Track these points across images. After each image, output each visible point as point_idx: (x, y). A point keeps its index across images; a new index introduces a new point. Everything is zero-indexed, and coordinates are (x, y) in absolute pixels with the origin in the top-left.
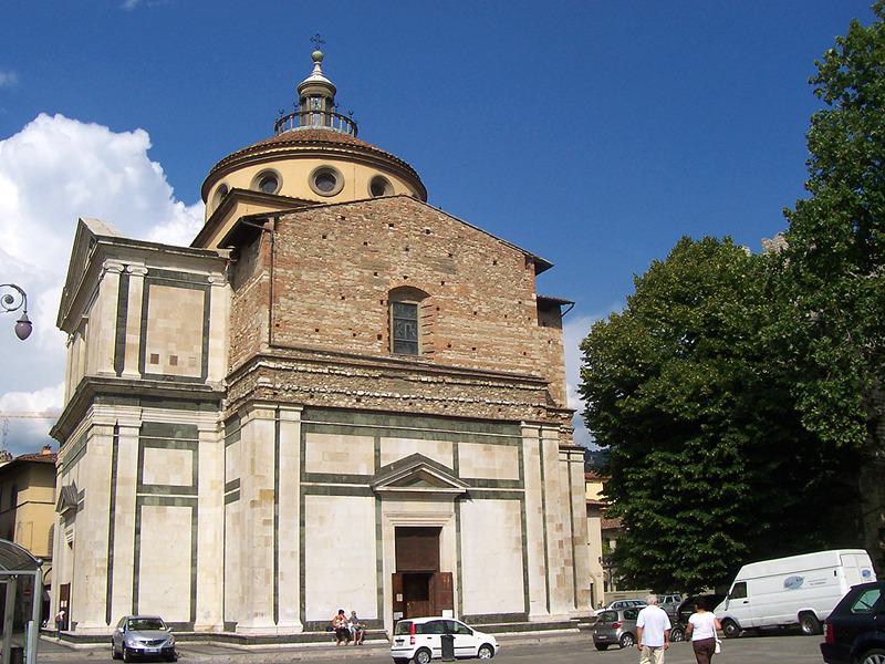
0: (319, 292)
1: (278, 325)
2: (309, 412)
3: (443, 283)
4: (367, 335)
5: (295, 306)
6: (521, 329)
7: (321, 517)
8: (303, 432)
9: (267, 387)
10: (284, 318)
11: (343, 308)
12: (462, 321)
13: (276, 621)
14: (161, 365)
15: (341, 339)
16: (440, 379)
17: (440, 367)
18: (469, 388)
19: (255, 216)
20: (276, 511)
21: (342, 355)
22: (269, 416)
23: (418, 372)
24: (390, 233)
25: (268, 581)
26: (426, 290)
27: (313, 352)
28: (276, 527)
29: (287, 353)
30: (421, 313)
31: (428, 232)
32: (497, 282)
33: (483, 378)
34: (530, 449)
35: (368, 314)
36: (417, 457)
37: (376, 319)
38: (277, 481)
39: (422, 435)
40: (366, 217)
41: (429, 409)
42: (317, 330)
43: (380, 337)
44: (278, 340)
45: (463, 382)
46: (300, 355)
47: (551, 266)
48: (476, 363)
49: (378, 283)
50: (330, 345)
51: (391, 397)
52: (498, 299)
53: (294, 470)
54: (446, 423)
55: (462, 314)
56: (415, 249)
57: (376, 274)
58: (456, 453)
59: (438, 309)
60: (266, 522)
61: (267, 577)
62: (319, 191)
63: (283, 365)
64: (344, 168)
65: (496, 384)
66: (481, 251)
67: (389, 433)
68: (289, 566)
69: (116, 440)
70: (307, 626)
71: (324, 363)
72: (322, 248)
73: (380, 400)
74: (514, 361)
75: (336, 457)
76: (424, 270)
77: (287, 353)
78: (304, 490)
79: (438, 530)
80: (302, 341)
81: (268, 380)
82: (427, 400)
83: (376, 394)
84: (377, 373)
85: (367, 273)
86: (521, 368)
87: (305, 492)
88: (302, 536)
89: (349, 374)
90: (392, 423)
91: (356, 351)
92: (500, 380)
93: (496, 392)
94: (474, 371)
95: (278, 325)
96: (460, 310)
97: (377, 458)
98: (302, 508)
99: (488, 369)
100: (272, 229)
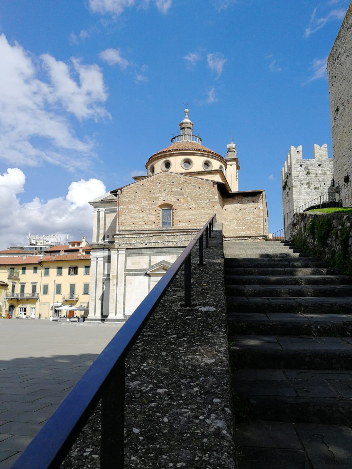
0: (134, 211)
3: (178, 200)
4: (150, 223)
6: (209, 211)
8: (126, 256)
9: (117, 244)
10: (123, 221)
11: (142, 215)
12: (185, 212)
14: (110, 238)
15: (141, 225)
16: (175, 234)
17: (176, 230)
18: (186, 236)
19: (114, 191)
20: (117, 281)
21: (142, 231)
22: (115, 253)
23: (166, 233)
27: (132, 231)
28: (117, 287)
29: (124, 233)
31: (173, 182)
32: (199, 195)
35: (151, 216)
39: (165, 254)
40: (151, 182)
41: (170, 245)
44: (121, 228)
45: (183, 234)
48: (190, 226)
52: (200, 202)
55: (185, 210)
57: (153, 202)
60: (114, 285)
63: (121, 236)
66: (194, 185)
67: (154, 254)
73: (153, 244)
76: (171, 196)
80: (129, 228)
81: (117, 242)
82: (170, 242)
83: (151, 242)
84: (152, 235)
85: (150, 202)
87: (126, 275)
88: (125, 289)
90: (155, 250)
94: (190, 229)
96: (184, 208)
98: (125, 280)
99: (195, 228)
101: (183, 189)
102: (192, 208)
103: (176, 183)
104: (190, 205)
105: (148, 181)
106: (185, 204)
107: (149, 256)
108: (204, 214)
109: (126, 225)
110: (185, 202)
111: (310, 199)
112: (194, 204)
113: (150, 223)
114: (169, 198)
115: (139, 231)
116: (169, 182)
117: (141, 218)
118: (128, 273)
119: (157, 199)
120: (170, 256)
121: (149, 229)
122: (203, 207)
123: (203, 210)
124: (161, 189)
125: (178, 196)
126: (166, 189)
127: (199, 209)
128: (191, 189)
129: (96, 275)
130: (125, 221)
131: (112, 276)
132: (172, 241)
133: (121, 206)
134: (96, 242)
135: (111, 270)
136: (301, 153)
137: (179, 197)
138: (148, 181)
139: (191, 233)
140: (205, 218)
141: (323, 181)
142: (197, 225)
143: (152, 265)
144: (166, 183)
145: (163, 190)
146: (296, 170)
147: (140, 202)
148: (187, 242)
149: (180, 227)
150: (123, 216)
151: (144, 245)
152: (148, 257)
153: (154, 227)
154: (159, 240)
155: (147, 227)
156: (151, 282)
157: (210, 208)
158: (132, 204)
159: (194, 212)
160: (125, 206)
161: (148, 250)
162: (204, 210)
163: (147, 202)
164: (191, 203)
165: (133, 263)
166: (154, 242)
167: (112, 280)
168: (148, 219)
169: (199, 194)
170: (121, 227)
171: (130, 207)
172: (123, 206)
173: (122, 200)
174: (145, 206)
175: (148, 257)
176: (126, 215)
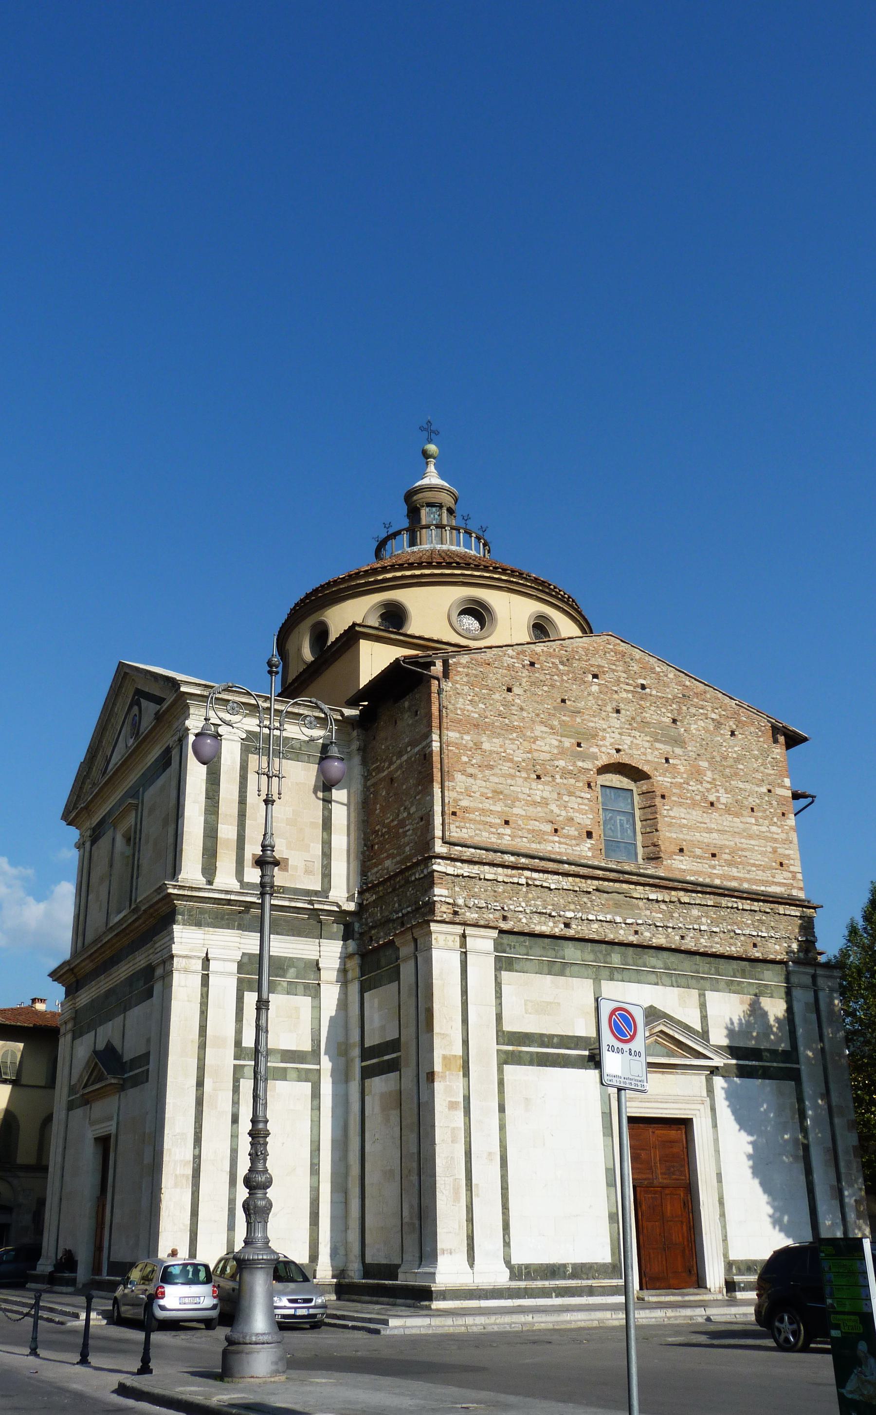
0: (506, 767)
1: (454, 814)
3: (667, 760)
4: (573, 832)
5: (477, 785)
6: (774, 829)
7: (527, 1099)
8: (498, 969)
10: (464, 803)
11: (540, 791)
12: (696, 815)
15: (538, 836)
18: (712, 912)
21: (541, 859)
22: (450, 944)
24: (595, 688)
25: (457, 1199)
26: (646, 768)
31: (643, 687)
32: (737, 760)
35: (573, 802)
38: (466, 1043)
40: (562, 663)
41: (660, 940)
42: (507, 822)
43: (589, 835)
44: (455, 833)
47: (805, 739)
49: (584, 757)
50: (524, 844)
52: (741, 785)
55: (694, 805)
57: (579, 745)
58: (703, 1006)
61: (456, 1191)
63: (466, 870)
64: (494, 598)
66: (714, 716)
67: (613, 974)
69: (205, 981)
70: (517, 1272)
72: (507, 704)
75: (543, 1008)
76: (642, 740)
77: (469, 853)
80: (486, 837)
81: (445, 892)
83: (591, 917)
87: (506, 1059)
88: (502, 1128)
90: (616, 959)
91: (560, 853)
93: (748, 919)
95: (454, 814)
96: (692, 798)
98: (501, 1083)
100: (440, 675)
102: (716, 804)
103: (654, 692)
105: (551, 655)
106: (691, 783)
107: (594, 979)
108: (759, 837)
112: (722, 791)
113: (573, 832)
116: (631, 682)
117: (535, 804)
118: (510, 1048)
119: (595, 736)
120: (676, 989)
121: (571, 859)
122: (752, 809)
127: (742, 815)
128: (706, 730)
129: (202, 1046)
130: (472, 805)
131: (445, 1057)
132: (667, 927)
133: (451, 734)
135: (436, 1029)
137: (668, 748)
138: (551, 655)
139: (730, 905)
140: (763, 854)
142: (741, 875)
144: (618, 682)
147: (529, 734)
148: (717, 939)
150: (459, 777)
151: (562, 926)
154: (616, 914)
157: (775, 820)
159: (728, 821)
160: (467, 737)
163: (556, 743)
164: (713, 782)
167: (444, 1078)
169: (735, 756)
170: (453, 827)
171: (486, 746)
172: (458, 735)
173: (450, 707)
174: (548, 756)
176: (471, 775)
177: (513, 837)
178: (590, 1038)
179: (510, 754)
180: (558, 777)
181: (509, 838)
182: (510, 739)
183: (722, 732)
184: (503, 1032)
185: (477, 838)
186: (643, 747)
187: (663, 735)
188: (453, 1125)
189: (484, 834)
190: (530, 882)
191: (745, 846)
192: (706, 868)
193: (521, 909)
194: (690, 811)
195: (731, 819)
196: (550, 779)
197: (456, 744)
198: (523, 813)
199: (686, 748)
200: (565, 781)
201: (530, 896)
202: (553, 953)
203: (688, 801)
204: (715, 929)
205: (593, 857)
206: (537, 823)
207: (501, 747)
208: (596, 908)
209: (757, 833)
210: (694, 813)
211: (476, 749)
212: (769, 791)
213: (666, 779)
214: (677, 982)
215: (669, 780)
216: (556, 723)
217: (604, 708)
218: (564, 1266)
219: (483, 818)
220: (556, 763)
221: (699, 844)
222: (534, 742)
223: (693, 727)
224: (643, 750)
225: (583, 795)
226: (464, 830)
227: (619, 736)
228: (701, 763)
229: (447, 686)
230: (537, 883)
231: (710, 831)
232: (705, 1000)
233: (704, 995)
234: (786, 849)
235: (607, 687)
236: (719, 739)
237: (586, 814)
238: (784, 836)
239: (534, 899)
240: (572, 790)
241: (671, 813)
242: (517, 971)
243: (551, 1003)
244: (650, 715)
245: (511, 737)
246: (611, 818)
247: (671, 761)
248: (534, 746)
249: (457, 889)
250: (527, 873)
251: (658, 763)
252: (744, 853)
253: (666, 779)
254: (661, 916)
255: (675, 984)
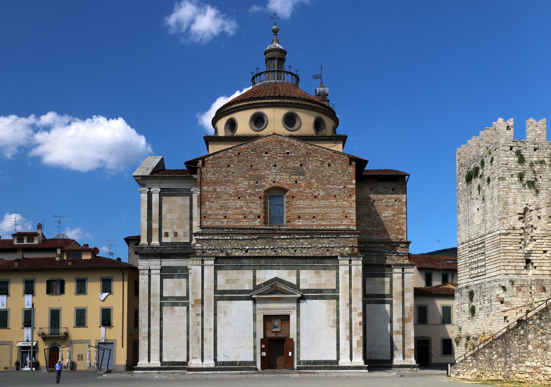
0: (226, 197)
1: (205, 217)
2: (219, 260)
3: (296, 182)
4: (252, 217)
5: (214, 205)
6: (344, 203)
9: (199, 249)
10: (208, 213)
11: (239, 203)
12: (307, 202)
13: (202, 361)
15: (238, 220)
21: (239, 229)
22: (198, 263)
26: (286, 187)
27: (223, 229)
29: (210, 231)
30: (285, 200)
33: (318, 234)
34: (343, 271)
35: (253, 206)
36: (276, 279)
37: (257, 208)
39: (278, 268)
41: (285, 253)
44: (205, 224)
46: (216, 231)
50: (232, 224)
51: (264, 249)
52: (331, 187)
53: (211, 289)
54: (294, 261)
55: (307, 198)
56: (279, 165)
57: (257, 183)
59: (293, 197)
62: (255, 128)
63: (207, 237)
65: (325, 236)
66: (321, 159)
67: (261, 267)
68: (209, 335)
71: (227, 234)
73: (258, 250)
74: (339, 222)
76: (285, 176)
78: (216, 299)
79: (288, 316)
80: (218, 224)
81: (199, 245)
82: (284, 248)
83: (256, 248)
85: (252, 183)
86: (344, 225)
87: (216, 300)
89: (241, 238)
90: (263, 262)
91: (246, 226)
92: (328, 234)
95: (205, 217)
96: (307, 196)
97: (254, 280)
99: (323, 227)
101: (305, 165)
104: (315, 191)
106: (307, 190)
108: (337, 207)
109: (212, 219)
110: (307, 186)
111: (521, 198)
112: (321, 190)
114: (283, 178)
115: (234, 229)
117: (236, 209)
119: (264, 178)
120: (287, 271)
121: (251, 227)
123: (335, 201)
124: (269, 162)
125: (295, 175)
126: (277, 163)
127: (329, 199)
128: (316, 166)
130: (212, 213)
134: (147, 243)
136: (512, 129)
137: (297, 177)
139: (317, 236)
140: (338, 214)
141: (539, 172)
142: (327, 224)
143: (258, 283)
144: (276, 154)
145: (271, 165)
146: (504, 155)
149: (300, 225)
150: (207, 203)
151: (244, 252)
152: (252, 271)
153: (259, 224)
154: (267, 245)
155: (247, 224)
156: (257, 311)
158: (222, 185)
159: (322, 203)
161: (252, 262)
162: (336, 200)
163: (247, 183)
164: (317, 188)
165: (227, 281)
166: (260, 247)
168: (249, 210)
169: (329, 174)
171: (218, 190)
172: (207, 188)
174: (243, 189)
175: (252, 271)
176: (212, 202)
177: (227, 222)
178: (250, 290)
179: (228, 191)
180: (247, 197)
181: (226, 223)
182: (228, 186)
183: (324, 165)
184: (217, 290)
185: (214, 225)
186: (285, 178)
187: (295, 172)
188: (197, 321)
189: (216, 222)
190: (232, 238)
191: (329, 212)
192: (310, 223)
193: (228, 248)
194: (305, 201)
195: (324, 202)
196: (244, 198)
197: (207, 191)
198: (232, 213)
199: (306, 176)
200: (250, 198)
201: (232, 243)
202: (238, 262)
203: (305, 197)
204: (309, 246)
205: (260, 225)
206: (238, 216)
207: (224, 189)
208: (259, 244)
209: (336, 205)
210: (307, 202)
211: (214, 192)
212: (344, 187)
213: (295, 190)
214: (288, 268)
215: (296, 190)
216: (247, 176)
217: (269, 166)
218: (236, 362)
219: (216, 217)
220: (247, 191)
221: (308, 214)
222: (238, 185)
223: (310, 166)
224: (285, 180)
225: (257, 202)
226: (208, 222)
227: (274, 176)
228: (312, 181)
229: (204, 170)
230: (234, 238)
231: (313, 208)
232: (299, 274)
233: (299, 272)
234: (350, 210)
235: (271, 156)
236: (322, 169)
237: (258, 209)
238: (349, 205)
239: (234, 244)
240: (253, 201)
241: (296, 203)
242: (223, 270)
243: (236, 279)
244: (291, 164)
245: (228, 184)
246: (274, 207)
247: (298, 182)
248: (238, 187)
249: (204, 244)
250: (231, 235)
251: (292, 184)
252: (329, 215)
253: (295, 190)
254: (286, 244)
255: (287, 268)
